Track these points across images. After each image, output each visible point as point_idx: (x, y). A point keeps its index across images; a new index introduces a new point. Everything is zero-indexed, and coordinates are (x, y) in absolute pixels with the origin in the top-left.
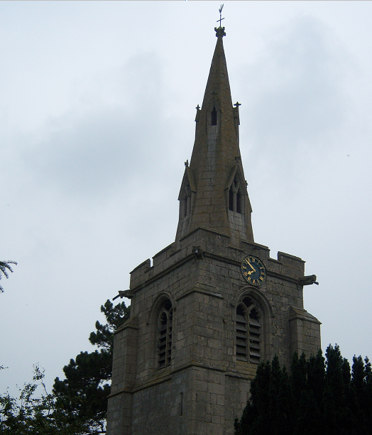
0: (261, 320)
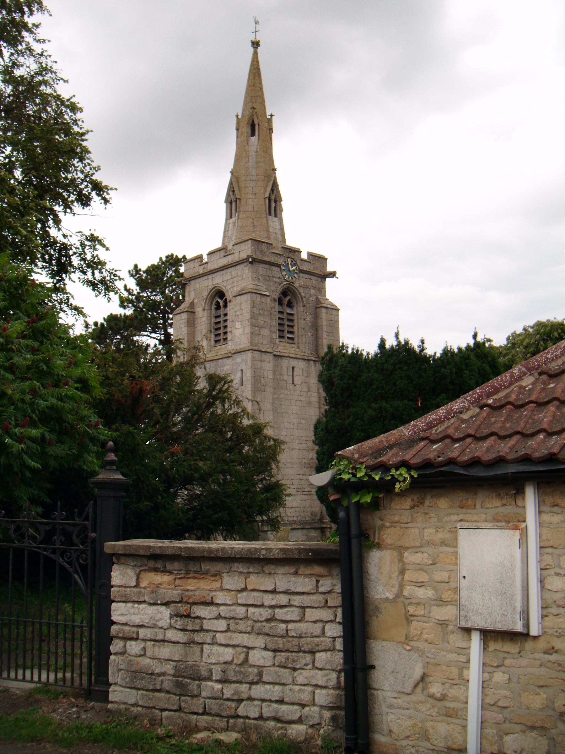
0: (295, 309)
